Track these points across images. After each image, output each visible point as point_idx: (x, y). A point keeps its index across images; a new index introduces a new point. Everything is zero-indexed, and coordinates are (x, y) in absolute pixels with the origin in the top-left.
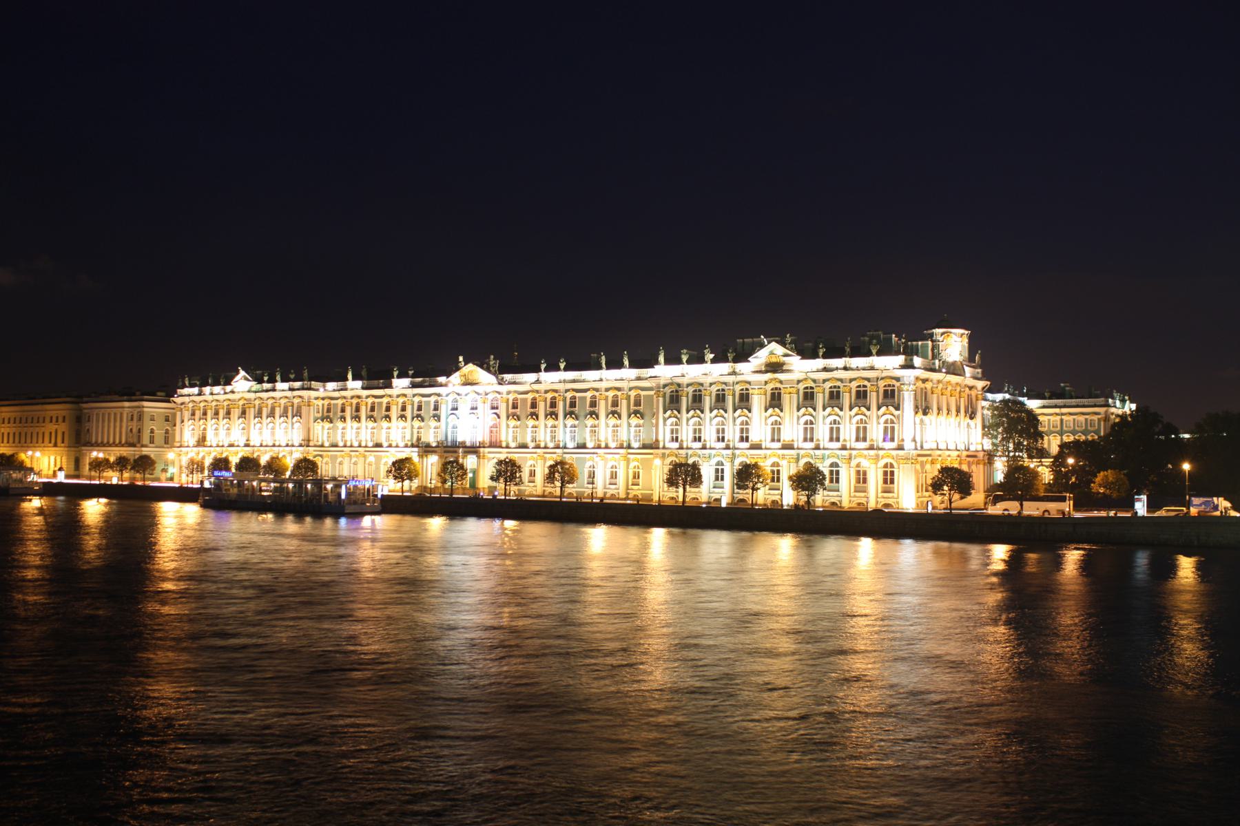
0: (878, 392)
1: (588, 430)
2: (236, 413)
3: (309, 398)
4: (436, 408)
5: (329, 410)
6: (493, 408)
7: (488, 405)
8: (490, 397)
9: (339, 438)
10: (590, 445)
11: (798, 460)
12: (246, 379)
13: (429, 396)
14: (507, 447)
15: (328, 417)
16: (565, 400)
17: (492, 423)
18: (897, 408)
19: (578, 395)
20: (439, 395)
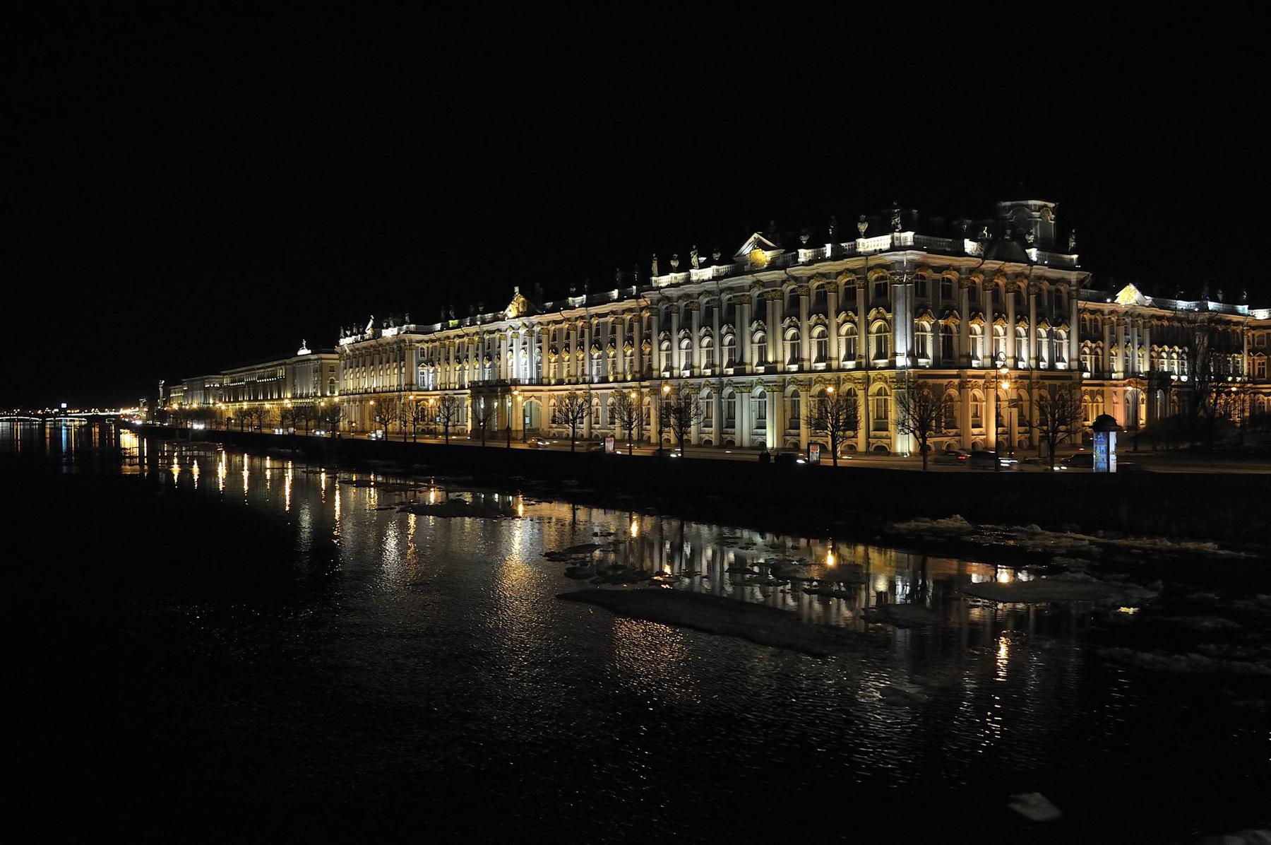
0: (866, 287)
1: (610, 360)
2: (368, 359)
3: (411, 341)
7: (534, 339)
10: (611, 379)
11: (783, 387)
14: (549, 384)
16: (590, 328)
18: (889, 311)
19: (602, 320)
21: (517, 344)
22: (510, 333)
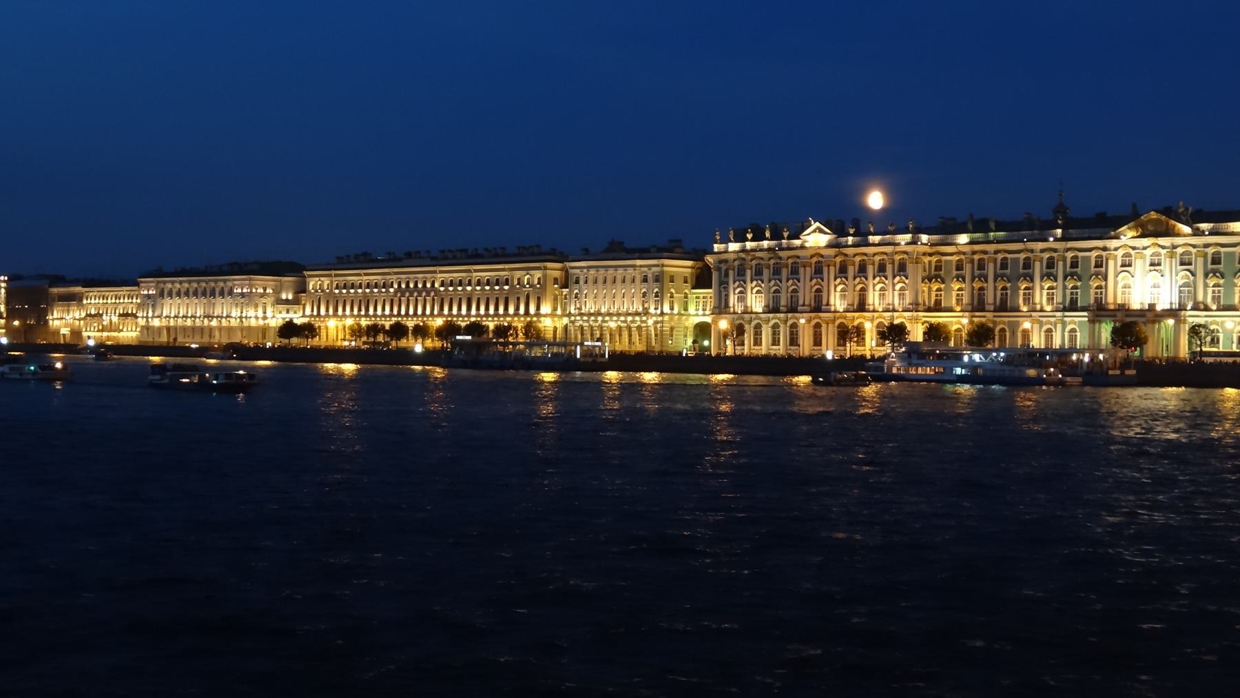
4: (1098, 265)
5: (938, 268)
6: (1182, 264)
8: (1180, 250)
9: (954, 301)
12: (821, 231)
13: (1090, 250)
15: (936, 277)
17: (1181, 282)
20: (1105, 249)
21: (1140, 266)
22: (1120, 253)
